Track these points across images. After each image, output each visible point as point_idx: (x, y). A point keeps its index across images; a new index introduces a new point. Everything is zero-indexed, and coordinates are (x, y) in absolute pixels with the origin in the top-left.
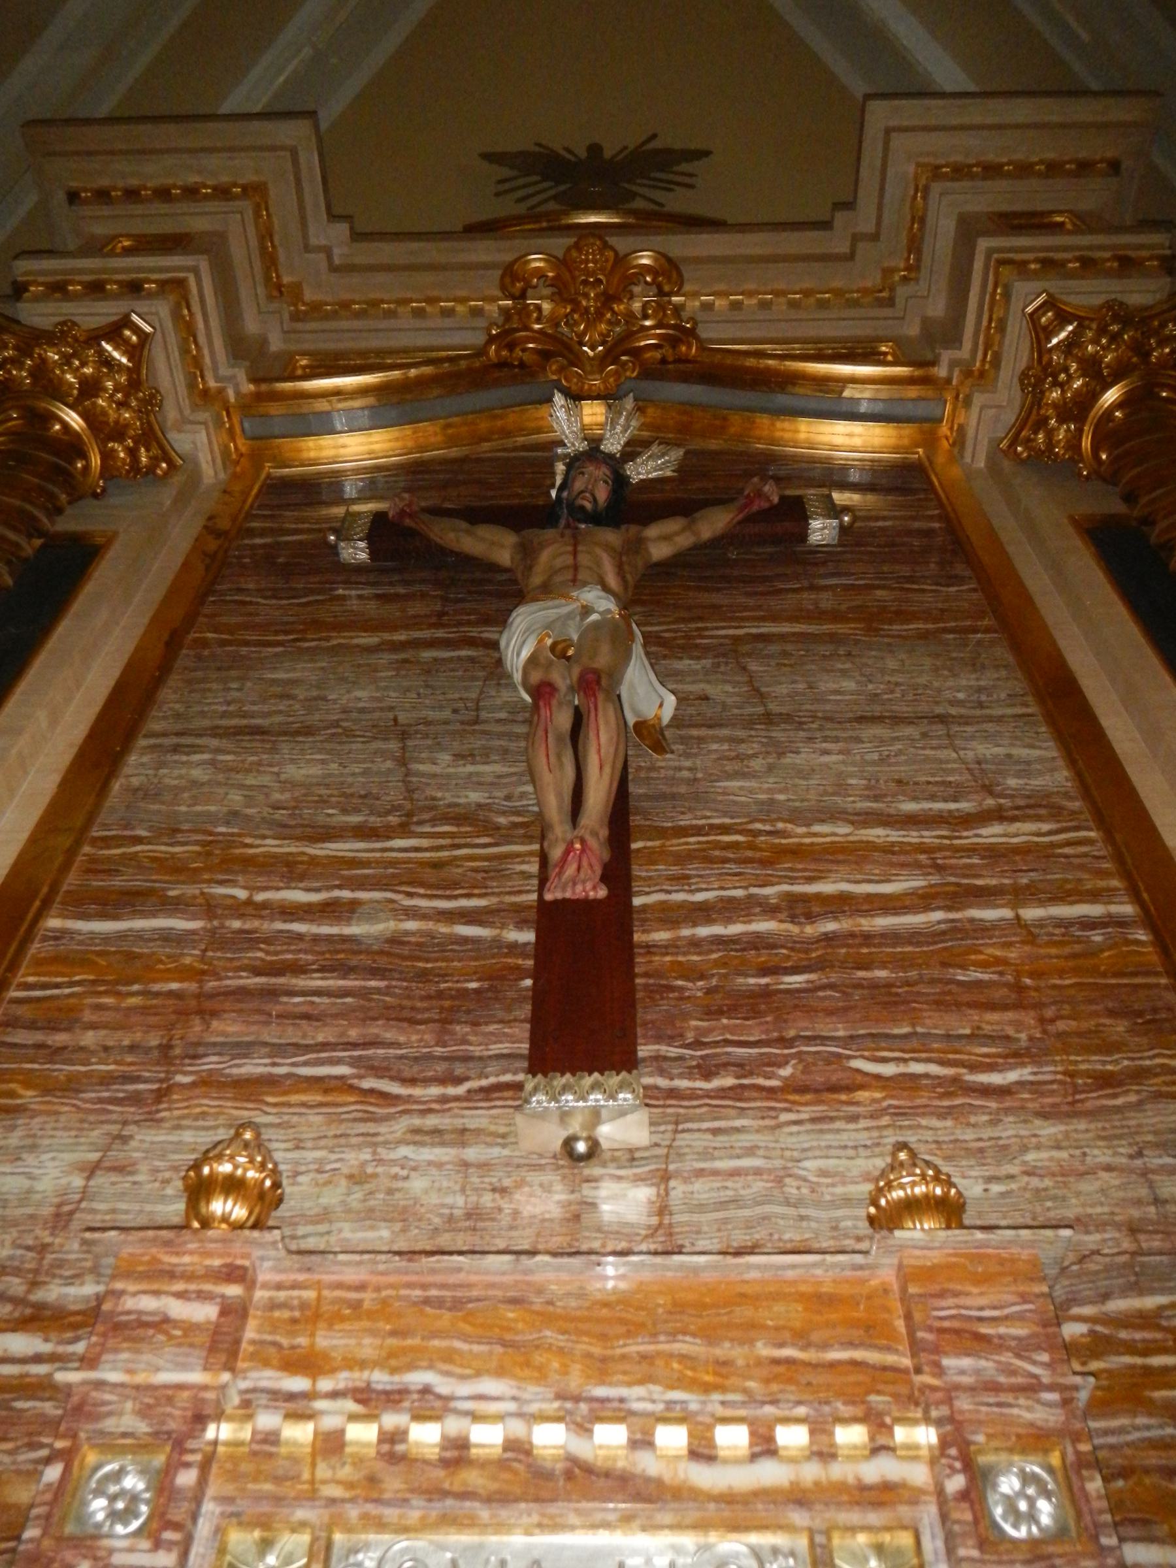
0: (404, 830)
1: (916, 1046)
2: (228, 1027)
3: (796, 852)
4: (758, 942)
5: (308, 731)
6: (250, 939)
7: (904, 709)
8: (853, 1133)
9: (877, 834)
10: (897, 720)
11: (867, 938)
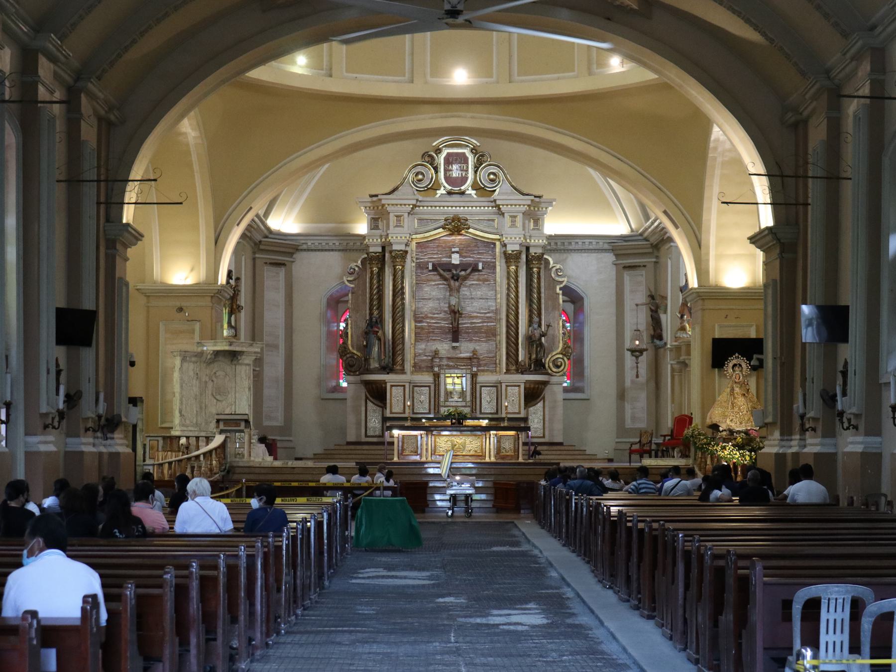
0: (440, 314)
1: (478, 337)
2: (431, 335)
3: (472, 317)
4: (468, 327)
5: (430, 299)
6: (430, 326)
7: (484, 297)
8: (472, 344)
9: (479, 315)
10: (484, 299)
11: (475, 326)
